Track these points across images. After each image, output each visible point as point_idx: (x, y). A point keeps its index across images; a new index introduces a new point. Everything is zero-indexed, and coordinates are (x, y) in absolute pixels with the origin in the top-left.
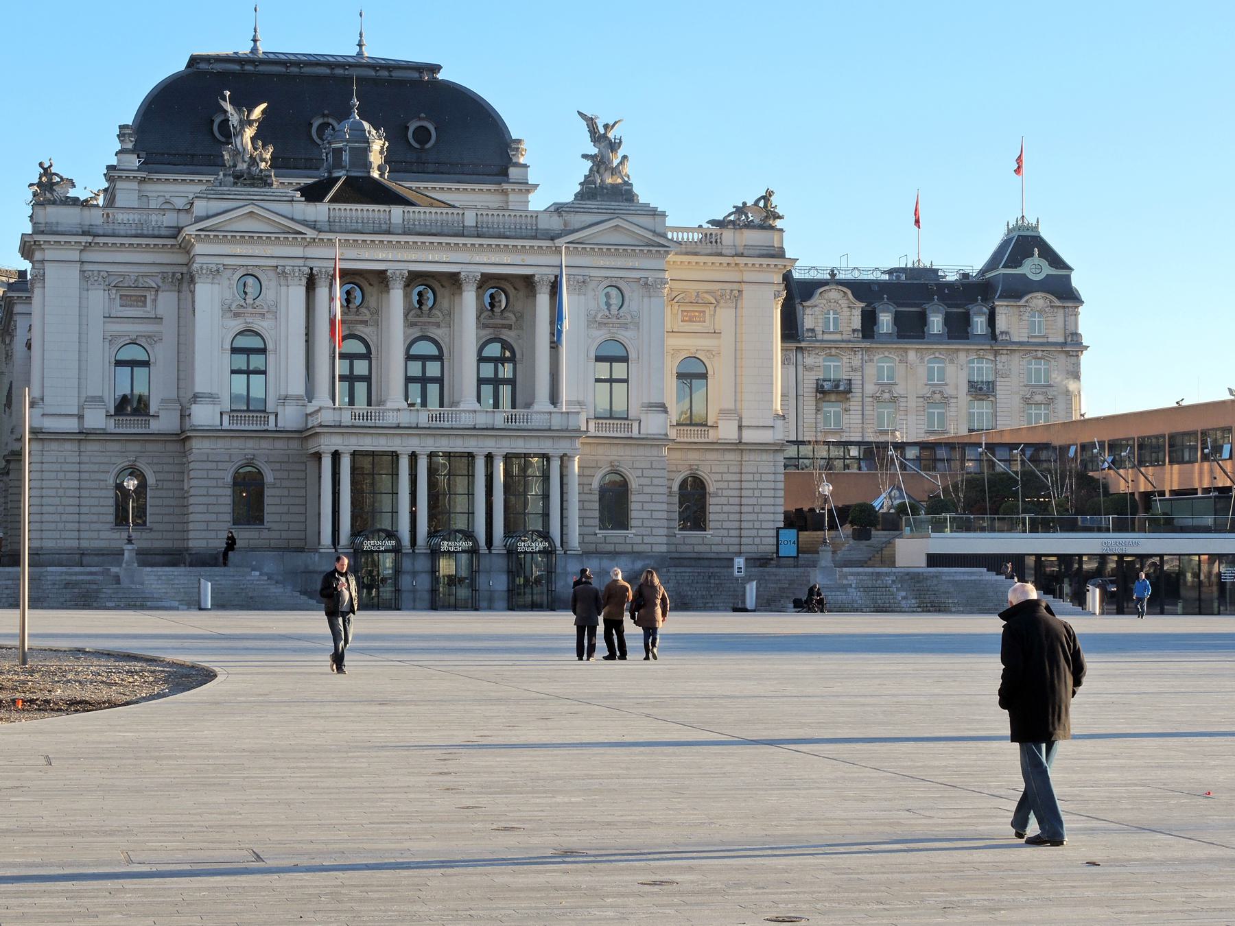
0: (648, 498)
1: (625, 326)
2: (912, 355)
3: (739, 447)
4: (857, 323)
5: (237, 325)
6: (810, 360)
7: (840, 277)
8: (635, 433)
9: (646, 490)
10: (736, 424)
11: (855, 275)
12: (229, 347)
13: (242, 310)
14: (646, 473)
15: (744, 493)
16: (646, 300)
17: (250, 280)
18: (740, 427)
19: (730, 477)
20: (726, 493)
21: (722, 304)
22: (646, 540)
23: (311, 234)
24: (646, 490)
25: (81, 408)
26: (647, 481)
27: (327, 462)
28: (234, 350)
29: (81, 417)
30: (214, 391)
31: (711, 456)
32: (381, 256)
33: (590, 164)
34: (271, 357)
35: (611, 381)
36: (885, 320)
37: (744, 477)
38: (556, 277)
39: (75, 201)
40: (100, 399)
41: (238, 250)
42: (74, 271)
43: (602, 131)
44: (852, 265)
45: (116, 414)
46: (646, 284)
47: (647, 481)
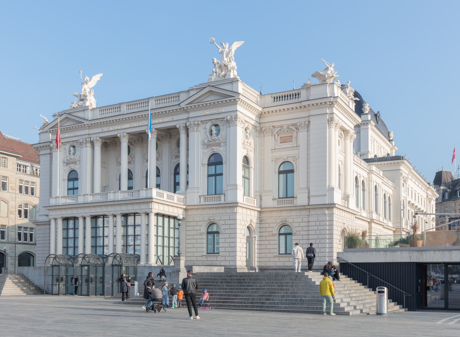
0: (227, 236)
1: (219, 145)
3: (308, 208)
8: (222, 201)
9: (227, 231)
10: (307, 194)
14: (227, 222)
15: (310, 233)
16: (228, 128)
19: (302, 224)
20: (301, 233)
21: (300, 130)
22: (227, 258)
23: (86, 123)
24: (227, 231)
26: (227, 227)
31: (294, 213)
32: (116, 128)
35: (216, 175)
37: (310, 224)
46: (227, 120)
47: (227, 227)
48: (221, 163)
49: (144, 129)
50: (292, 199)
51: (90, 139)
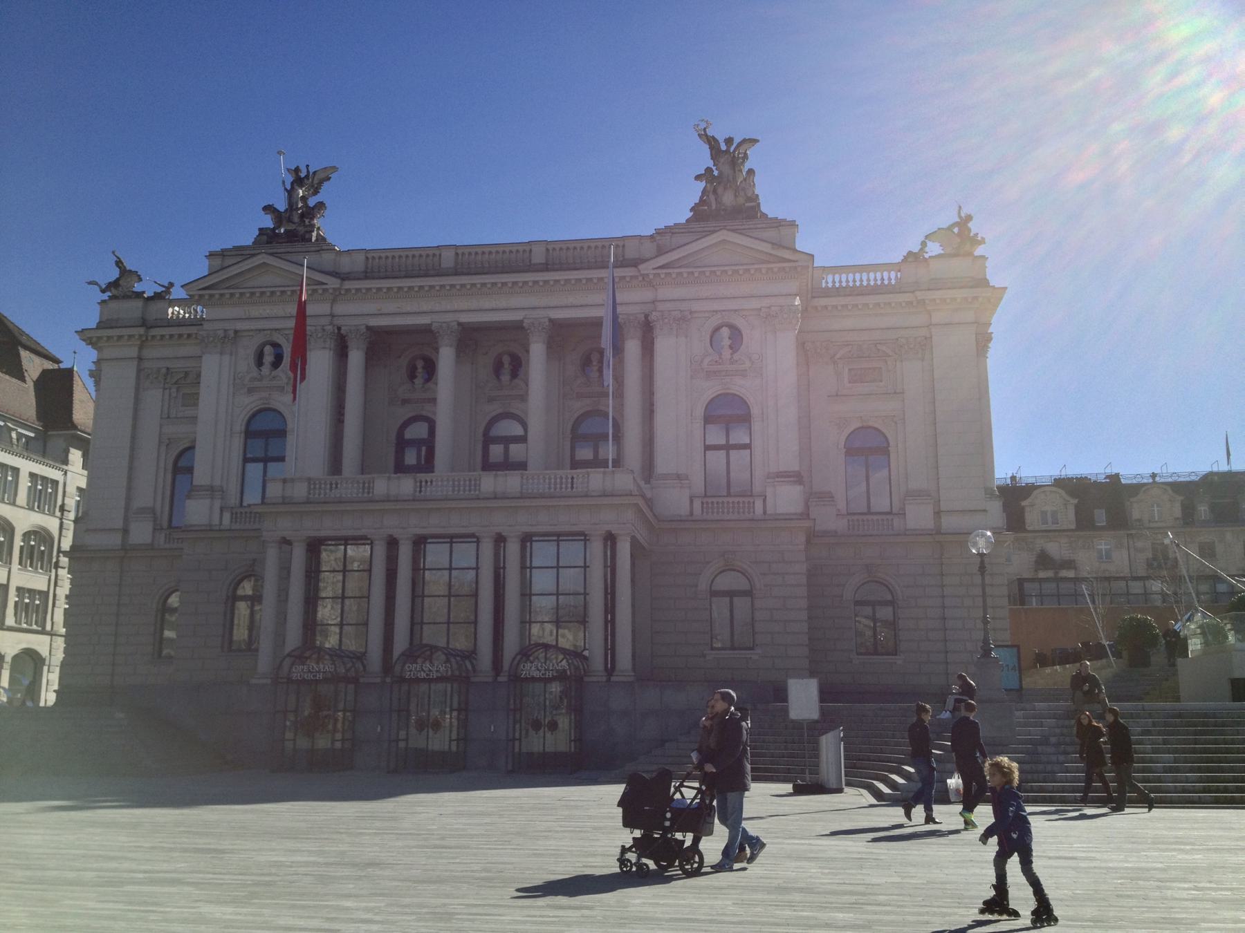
2: (1229, 536)
4: (1177, 511)
5: (250, 403)
6: (1139, 544)
7: (1157, 479)
11: (1175, 478)
12: (239, 426)
13: (257, 384)
17: (268, 349)
18: (938, 514)
25: (126, 519)
27: (272, 557)
28: (249, 434)
29: (126, 531)
30: (217, 482)
33: (701, 185)
34: (291, 439)
36: (1203, 510)
38: (646, 316)
39: (139, 295)
40: (153, 511)
41: (255, 311)
42: (130, 371)
43: (723, 147)
44: (1171, 470)
45: (170, 526)
48: (745, 418)
49: (518, 318)
50: (889, 517)
51: (339, 329)
